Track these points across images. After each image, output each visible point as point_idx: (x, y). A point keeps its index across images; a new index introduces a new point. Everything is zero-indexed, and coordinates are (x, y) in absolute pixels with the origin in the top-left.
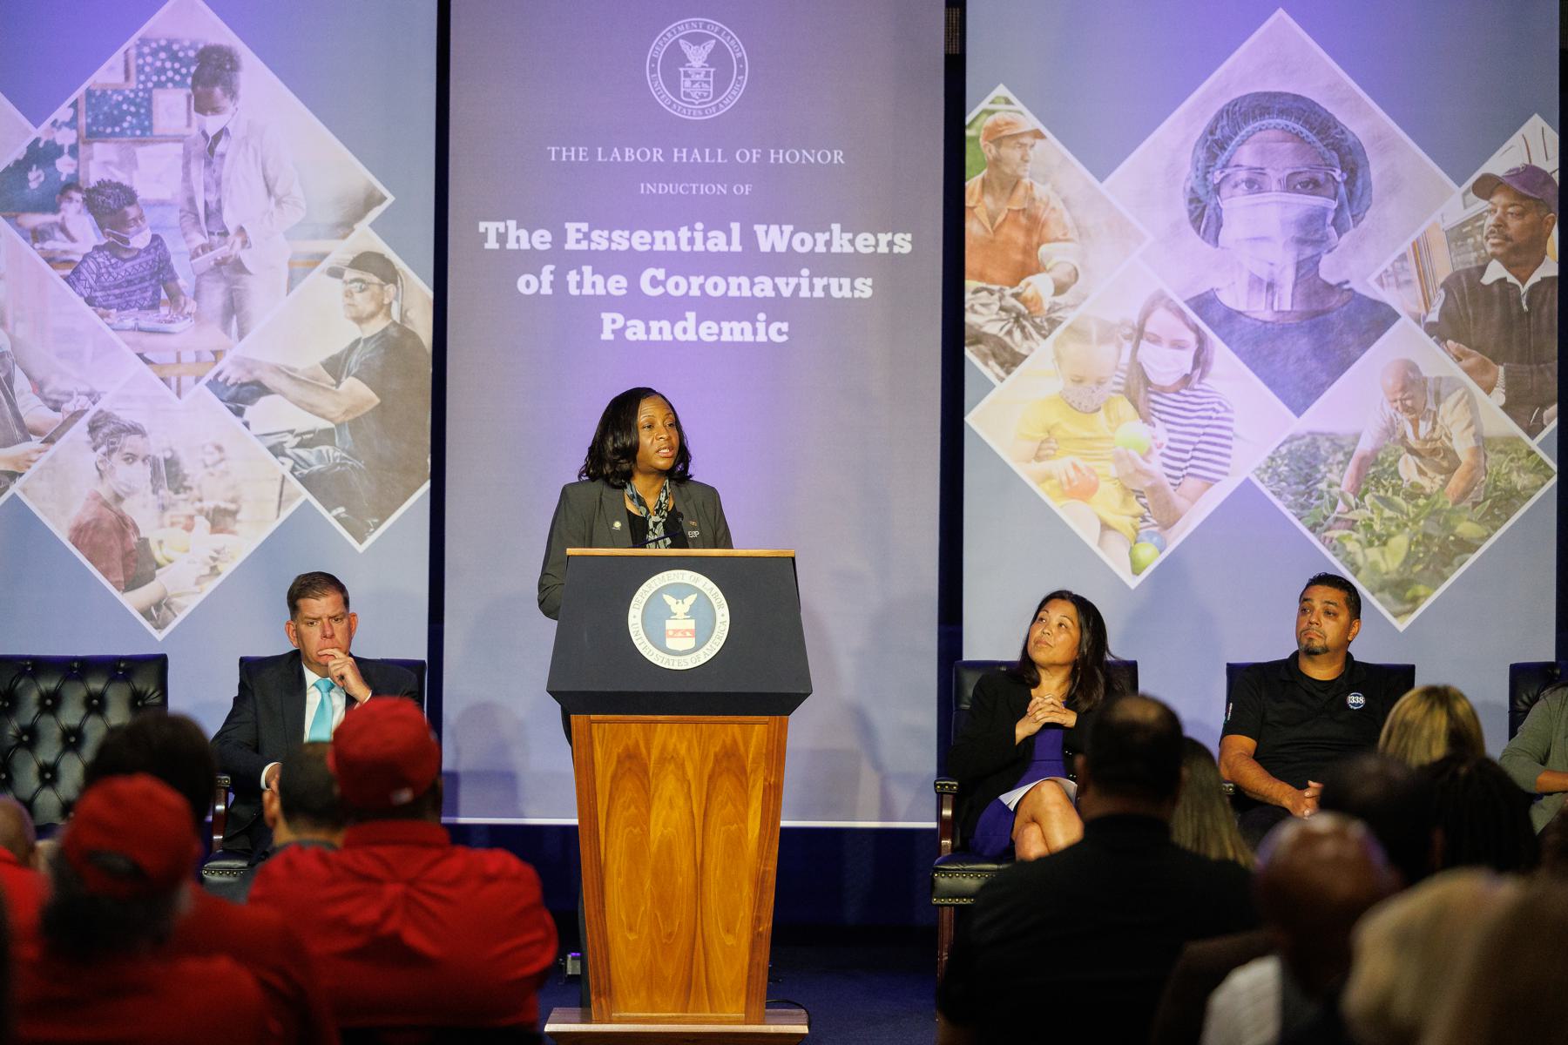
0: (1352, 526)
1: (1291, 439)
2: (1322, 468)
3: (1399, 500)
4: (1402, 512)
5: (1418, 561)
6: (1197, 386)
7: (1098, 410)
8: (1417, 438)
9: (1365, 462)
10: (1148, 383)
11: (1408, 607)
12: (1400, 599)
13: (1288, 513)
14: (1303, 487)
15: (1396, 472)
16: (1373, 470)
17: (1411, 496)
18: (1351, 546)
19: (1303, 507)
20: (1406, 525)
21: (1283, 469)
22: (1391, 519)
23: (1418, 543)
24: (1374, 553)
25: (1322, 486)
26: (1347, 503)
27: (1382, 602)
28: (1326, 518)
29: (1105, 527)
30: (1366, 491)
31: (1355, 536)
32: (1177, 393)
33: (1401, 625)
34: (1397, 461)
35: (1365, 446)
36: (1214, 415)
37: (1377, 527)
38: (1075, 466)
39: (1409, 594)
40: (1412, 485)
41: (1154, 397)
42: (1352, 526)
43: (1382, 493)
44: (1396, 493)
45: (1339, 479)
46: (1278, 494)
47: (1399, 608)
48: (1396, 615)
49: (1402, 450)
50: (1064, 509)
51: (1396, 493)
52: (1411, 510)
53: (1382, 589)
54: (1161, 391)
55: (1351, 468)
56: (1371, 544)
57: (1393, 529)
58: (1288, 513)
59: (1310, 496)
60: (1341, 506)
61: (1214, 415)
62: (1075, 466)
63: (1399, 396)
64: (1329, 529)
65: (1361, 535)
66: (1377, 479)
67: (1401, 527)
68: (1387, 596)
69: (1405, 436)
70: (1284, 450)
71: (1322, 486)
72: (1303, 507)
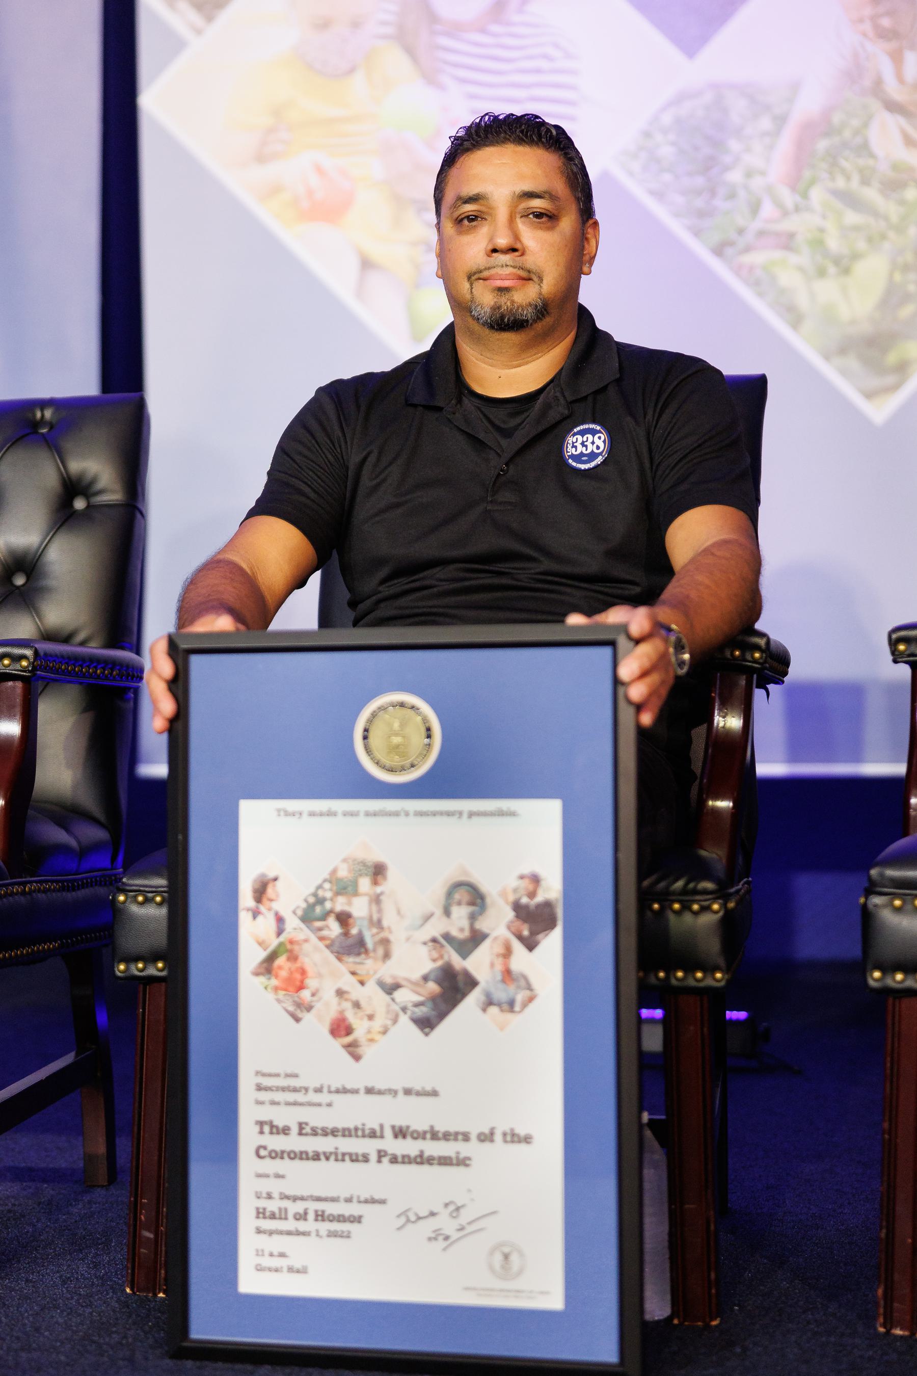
0: (787, 242)
1: (680, 98)
2: (734, 145)
3: (872, 194)
4: (875, 214)
5: (907, 298)
6: (516, 18)
7: (352, 71)
8: (900, 79)
9: (813, 129)
10: (432, 17)
11: (890, 380)
12: (875, 365)
13: (678, 228)
14: (700, 181)
15: (864, 149)
16: (822, 145)
17: (893, 186)
18: (788, 278)
19: (702, 214)
20: (883, 237)
21: (667, 151)
22: (856, 228)
23: (906, 268)
24: (828, 290)
25: (735, 177)
26: (778, 204)
27: (844, 372)
28: (741, 231)
29: (366, 264)
30: (812, 182)
31: (794, 259)
32: (483, 31)
33: (879, 412)
34: (866, 125)
35: (809, 104)
36: (544, 64)
37: (833, 243)
38: (320, 170)
39: (892, 358)
40: (895, 167)
41: (444, 41)
42: (787, 242)
43: (841, 183)
44: (865, 182)
45: (760, 162)
46: (659, 195)
47: (875, 382)
48: (869, 395)
49: (875, 105)
50: (304, 242)
51: (865, 182)
52: (893, 210)
53: (843, 351)
54: (455, 29)
55: (785, 144)
56: (822, 273)
57: (862, 245)
58: (678, 228)
59: (713, 193)
60: (768, 210)
61: (544, 64)
62: (320, 170)
63: (868, 11)
64: (748, 249)
65: (803, 258)
66: (833, 159)
67: (875, 240)
68: (852, 362)
69: (878, 82)
70: (667, 119)
71: (735, 177)
72: (702, 214)
